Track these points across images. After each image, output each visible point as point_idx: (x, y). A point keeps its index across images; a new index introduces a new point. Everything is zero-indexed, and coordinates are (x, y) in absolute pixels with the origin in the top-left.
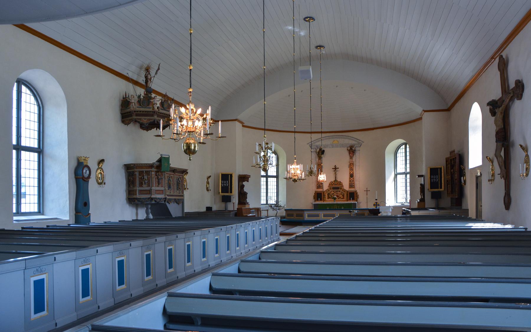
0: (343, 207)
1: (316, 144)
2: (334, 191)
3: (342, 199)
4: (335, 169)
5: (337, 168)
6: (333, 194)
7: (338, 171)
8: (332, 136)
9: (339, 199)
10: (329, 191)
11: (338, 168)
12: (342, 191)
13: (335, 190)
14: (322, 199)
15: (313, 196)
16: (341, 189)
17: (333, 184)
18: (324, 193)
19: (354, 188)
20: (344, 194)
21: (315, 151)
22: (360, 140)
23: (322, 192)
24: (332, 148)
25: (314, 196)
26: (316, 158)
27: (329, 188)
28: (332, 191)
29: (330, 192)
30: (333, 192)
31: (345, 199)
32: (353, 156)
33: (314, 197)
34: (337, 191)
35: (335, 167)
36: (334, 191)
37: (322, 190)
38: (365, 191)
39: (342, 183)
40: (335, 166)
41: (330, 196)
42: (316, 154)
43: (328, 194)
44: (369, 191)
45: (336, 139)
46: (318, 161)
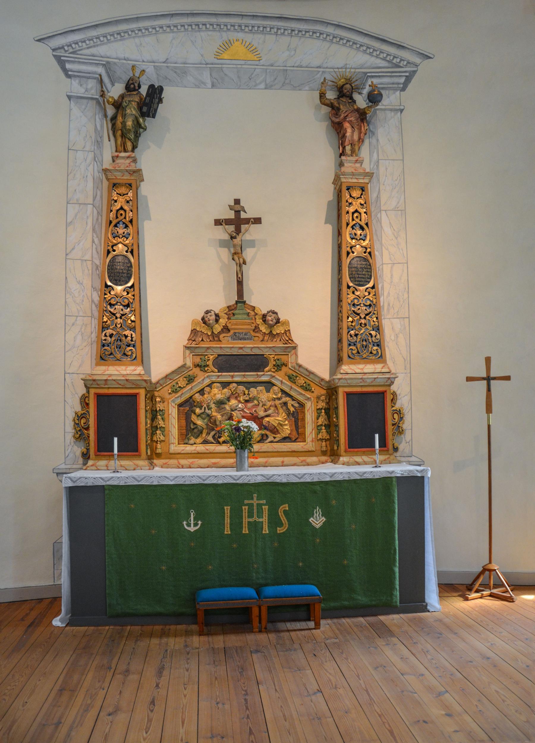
0: (318, 512)
1: (103, 50)
2: (225, 385)
3: (285, 439)
4: (232, 228)
5: (247, 221)
6: (220, 403)
7: (252, 244)
8: (216, 15)
9: (263, 439)
10: (190, 380)
11: (258, 221)
12: (287, 385)
13: (238, 376)
14: (143, 446)
15: (71, 416)
16: (278, 367)
17: (218, 328)
18: (151, 398)
19: (381, 358)
20: (302, 405)
21: (95, 93)
22: (400, 47)
23: (135, 384)
24: (213, 86)
25: (80, 417)
26: (99, 143)
27: (189, 363)
28: (210, 385)
29: (202, 392)
30: (218, 393)
31: (309, 443)
32: (361, 140)
33: (76, 424)
34: (249, 385)
35: (237, 212)
36: (225, 385)
37: (139, 370)
38: (469, 379)
39: (287, 323)
40: (237, 201)
41: (199, 422)
42: (99, 117)
43: (180, 405)
44: (508, 378)
45: (241, 35)
46: (114, 159)
